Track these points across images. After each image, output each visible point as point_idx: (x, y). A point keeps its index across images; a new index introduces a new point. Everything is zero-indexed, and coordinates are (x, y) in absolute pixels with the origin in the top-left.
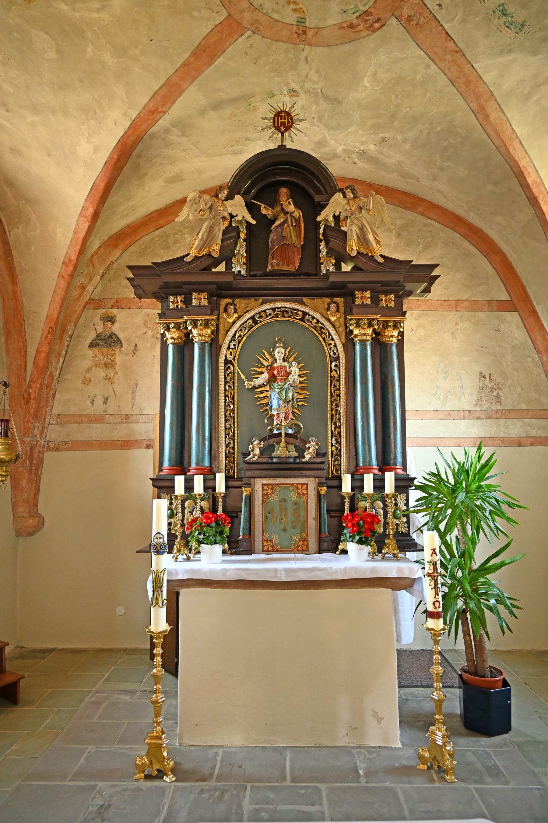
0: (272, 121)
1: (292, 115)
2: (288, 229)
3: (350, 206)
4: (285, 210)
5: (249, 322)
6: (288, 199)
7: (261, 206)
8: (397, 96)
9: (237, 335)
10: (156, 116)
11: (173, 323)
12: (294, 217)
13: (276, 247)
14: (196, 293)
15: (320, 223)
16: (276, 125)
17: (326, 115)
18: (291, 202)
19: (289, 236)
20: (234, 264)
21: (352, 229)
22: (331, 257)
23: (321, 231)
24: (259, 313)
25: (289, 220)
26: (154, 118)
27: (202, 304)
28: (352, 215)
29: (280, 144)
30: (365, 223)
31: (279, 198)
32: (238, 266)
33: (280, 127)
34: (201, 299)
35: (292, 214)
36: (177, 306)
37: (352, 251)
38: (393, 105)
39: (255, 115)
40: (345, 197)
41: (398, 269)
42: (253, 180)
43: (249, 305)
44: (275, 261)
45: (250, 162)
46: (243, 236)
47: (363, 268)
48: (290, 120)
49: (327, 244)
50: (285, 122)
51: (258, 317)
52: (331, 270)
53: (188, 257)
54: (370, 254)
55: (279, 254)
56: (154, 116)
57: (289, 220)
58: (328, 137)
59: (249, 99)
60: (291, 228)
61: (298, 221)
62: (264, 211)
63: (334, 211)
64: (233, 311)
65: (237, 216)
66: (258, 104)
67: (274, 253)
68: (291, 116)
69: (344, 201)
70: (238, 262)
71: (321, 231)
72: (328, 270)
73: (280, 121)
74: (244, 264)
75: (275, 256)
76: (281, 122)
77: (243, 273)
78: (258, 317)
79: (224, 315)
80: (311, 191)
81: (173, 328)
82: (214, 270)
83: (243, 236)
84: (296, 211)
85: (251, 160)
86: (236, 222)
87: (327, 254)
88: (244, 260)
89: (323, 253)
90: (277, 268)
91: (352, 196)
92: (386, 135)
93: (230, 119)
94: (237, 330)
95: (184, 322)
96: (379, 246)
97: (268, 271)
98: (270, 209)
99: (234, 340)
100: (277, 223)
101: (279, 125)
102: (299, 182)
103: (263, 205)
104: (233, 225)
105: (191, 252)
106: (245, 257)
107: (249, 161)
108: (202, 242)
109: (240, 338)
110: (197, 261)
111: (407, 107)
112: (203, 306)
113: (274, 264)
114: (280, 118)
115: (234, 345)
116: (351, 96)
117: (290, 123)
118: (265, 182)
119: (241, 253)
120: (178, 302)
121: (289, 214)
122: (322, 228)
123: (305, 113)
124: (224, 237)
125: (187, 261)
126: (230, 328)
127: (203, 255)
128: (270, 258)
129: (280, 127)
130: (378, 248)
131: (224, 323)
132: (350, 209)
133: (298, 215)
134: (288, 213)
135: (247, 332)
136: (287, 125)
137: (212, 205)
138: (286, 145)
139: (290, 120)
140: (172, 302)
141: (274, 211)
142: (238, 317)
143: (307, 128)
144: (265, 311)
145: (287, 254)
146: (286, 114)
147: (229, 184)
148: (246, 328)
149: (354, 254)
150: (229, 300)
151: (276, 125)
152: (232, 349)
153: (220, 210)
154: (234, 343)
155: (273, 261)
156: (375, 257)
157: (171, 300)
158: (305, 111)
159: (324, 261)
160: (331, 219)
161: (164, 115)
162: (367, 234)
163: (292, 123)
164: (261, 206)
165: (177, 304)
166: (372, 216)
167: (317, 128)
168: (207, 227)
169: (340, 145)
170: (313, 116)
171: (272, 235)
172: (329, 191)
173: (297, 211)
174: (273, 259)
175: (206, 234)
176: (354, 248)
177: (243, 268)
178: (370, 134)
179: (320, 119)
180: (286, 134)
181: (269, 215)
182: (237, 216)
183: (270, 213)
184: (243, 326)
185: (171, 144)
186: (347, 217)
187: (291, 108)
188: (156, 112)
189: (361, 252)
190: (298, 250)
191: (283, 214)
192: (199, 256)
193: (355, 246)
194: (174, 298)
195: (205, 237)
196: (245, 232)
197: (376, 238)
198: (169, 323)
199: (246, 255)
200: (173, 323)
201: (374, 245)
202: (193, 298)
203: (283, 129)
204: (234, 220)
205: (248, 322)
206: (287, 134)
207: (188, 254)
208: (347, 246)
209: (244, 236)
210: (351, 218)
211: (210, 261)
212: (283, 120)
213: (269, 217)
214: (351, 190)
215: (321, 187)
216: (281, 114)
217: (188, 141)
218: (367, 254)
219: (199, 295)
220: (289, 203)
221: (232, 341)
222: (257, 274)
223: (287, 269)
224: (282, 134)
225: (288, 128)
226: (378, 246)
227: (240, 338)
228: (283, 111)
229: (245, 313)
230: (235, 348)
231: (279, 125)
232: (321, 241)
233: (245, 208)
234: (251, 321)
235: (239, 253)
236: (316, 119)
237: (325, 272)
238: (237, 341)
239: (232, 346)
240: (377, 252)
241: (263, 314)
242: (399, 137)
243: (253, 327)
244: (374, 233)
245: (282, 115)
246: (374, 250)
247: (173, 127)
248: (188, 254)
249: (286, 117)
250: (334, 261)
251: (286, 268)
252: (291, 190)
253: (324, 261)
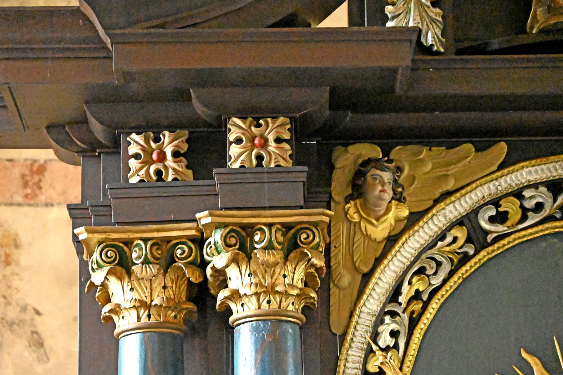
5: (455, 239)
9: (407, 292)
11: (145, 240)
14: (243, 118)
24: (496, 203)
27: (270, 164)
34: (265, 144)
36: (158, 173)
43: (453, 170)
51: (492, 220)
64: (388, 195)
78: (492, 220)
79: (352, 211)
81: (146, 262)
94: (405, 273)
95: (193, 239)
99: (393, 314)
109: (417, 306)
112: (270, 172)
115: (394, 334)
120: (162, 157)
126: (378, 261)
131: (351, 243)
135: (445, 281)
140: (137, 156)
142: (408, 218)
144: (518, 194)
148: (439, 264)
150: (375, 152)
152: (387, 349)
154: (394, 326)
157: (133, 149)
165: (160, 166)
184: (429, 253)
194: (147, 141)
198: (128, 243)
200: (145, 240)
202: (232, 137)
205: (449, 239)
219: (258, 125)
221: (387, 319)
227: (417, 306)
229: (437, 201)
230: (396, 346)
234: (461, 233)
238: (406, 317)
239: (385, 340)
241: (506, 205)
243: (465, 258)
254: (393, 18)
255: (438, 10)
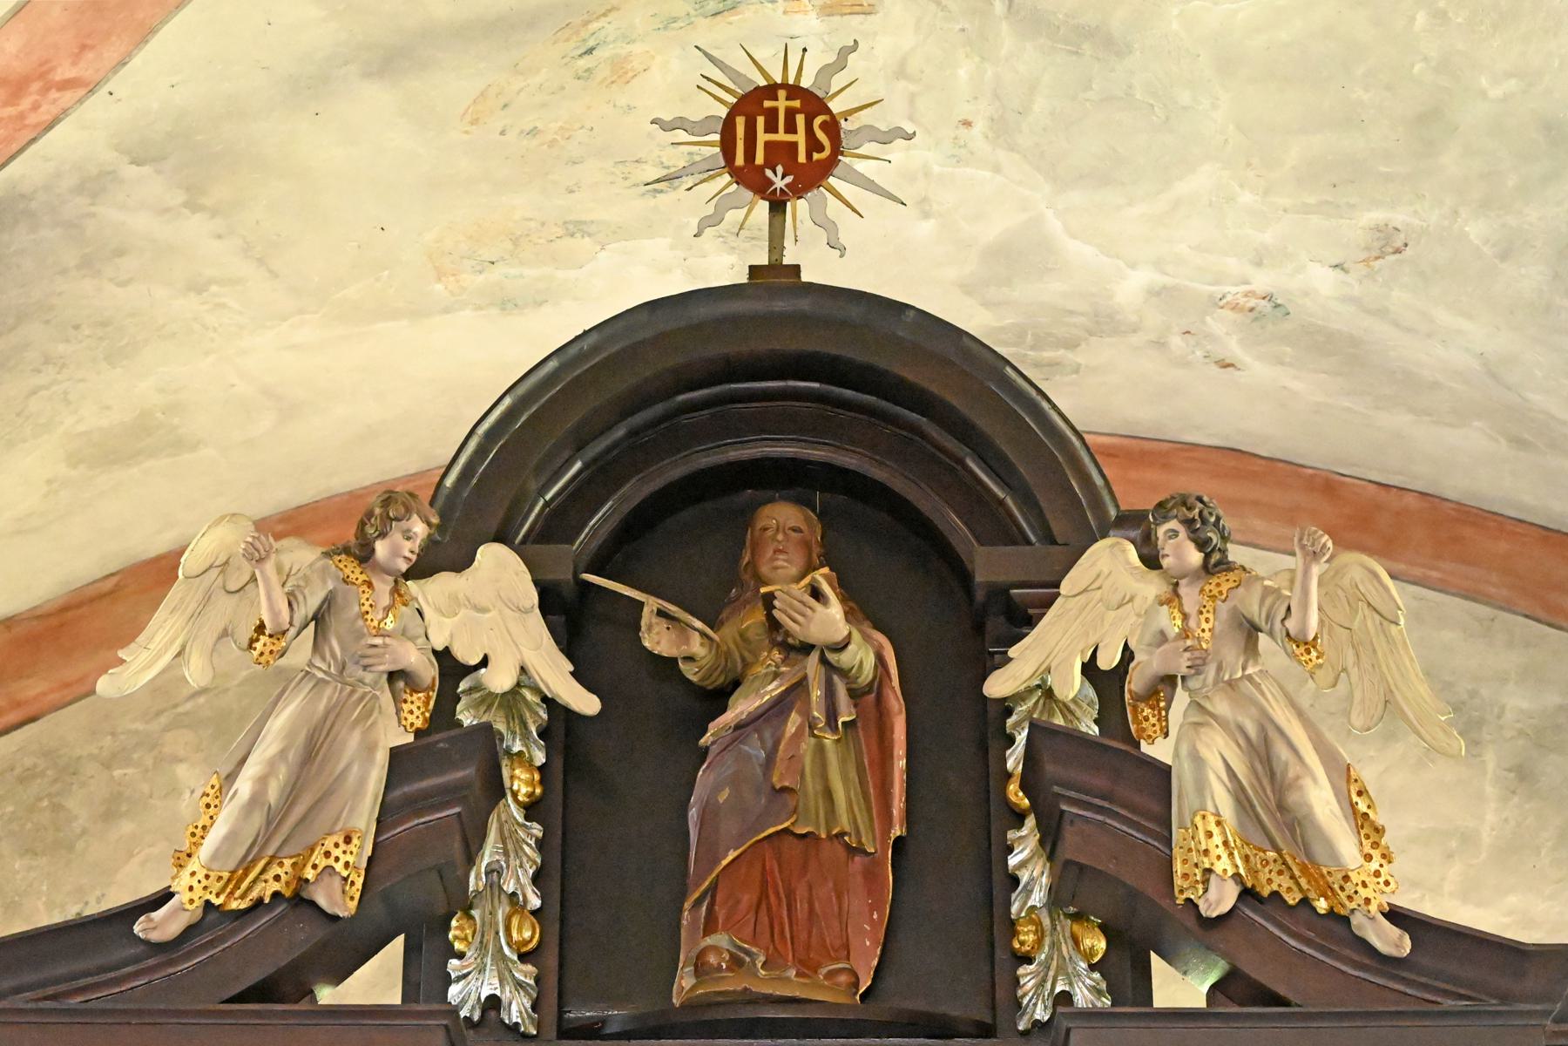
0: (717, 137)
1: (835, 106)
2: (807, 745)
3: (1185, 617)
4: (787, 634)
6: (810, 568)
7: (641, 605)
8: (1440, 16)
10: (35, 107)
12: (844, 673)
13: (732, 855)
15: (1009, 712)
16: (740, 160)
17: (1036, 108)
18: (826, 588)
19: (812, 785)
20: (461, 956)
21: (1204, 752)
22: (1077, 917)
23: (1014, 759)
25: (817, 693)
26: (22, 116)
28: (1197, 668)
29: (763, 260)
30: (1282, 716)
31: (753, 564)
32: (481, 970)
33: (761, 169)
35: (832, 657)
37: (1206, 882)
38: (1425, 59)
39: (623, 101)
40: (1151, 561)
41: (1504, 998)
42: (595, 460)
44: (721, 939)
45: (582, 357)
46: (522, 783)
47: (1282, 990)
48: (821, 136)
49: (1050, 841)
50: (794, 145)
52: (1083, 997)
53: (157, 915)
54: (1322, 905)
55: (747, 898)
56: (26, 104)
57: (817, 693)
58: (1054, 225)
59: (586, 23)
60: (829, 739)
61: (868, 695)
62: (657, 639)
63: (1092, 640)
65: (484, 662)
66: (637, 48)
67: (713, 888)
68: (828, 111)
69: (1151, 587)
70: (483, 946)
71: (1014, 759)
72: (1065, 998)
73: (762, 137)
74: (523, 957)
75: (721, 914)
76: (767, 144)
77: (517, 1010)
80: (953, 524)
82: (326, 995)
83: (522, 783)
84: (856, 636)
85: (585, 345)
86: (483, 700)
87: (1056, 899)
88: (527, 933)
89: (1028, 892)
90: (732, 984)
91: (1195, 557)
92: (1399, 217)
93: (474, 122)
96: (1376, 854)
97: (676, 1001)
98: (698, 624)
100: (741, 707)
101: (760, 159)
102: (878, 474)
103: (651, 604)
104: (466, 717)
105: (180, 885)
106: (534, 913)
107: (573, 351)
108: (258, 820)
110: (222, 939)
111: (1509, 75)
113: (712, 959)
114: (761, 121)
116: (1175, 11)
117: (821, 149)
118: (674, 470)
119: (510, 887)
121: (814, 657)
122: (1021, 738)
123: (912, 99)
124: (397, 793)
125: (155, 936)
127: (259, 903)
128: (694, 921)
129: (761, 169)
130: (1374, 866)
132: (1185, 633)
133: (870, 661)
134: (806, 648)
136: (802, 158)
137: (329, 602)
138: (796, 269)
139: (821, 136)
141: (728, 633)
143: (927, 174)
145: (801, 892)
146: (797, 104)
147: (449, 481)
149: (1220, 899)
151: (740, 160)
153: (380, 633)
155: (709, 941)
156: (1357, 920)
158: (912, 87)
159: (1039, 942)
160: (1071, 684)
161: (80, 101)
162: (1295, 784)
163: (837, 150)
164: (641, 605)
166: (1324, 676)
167: (988, 174)
168: (290, 735)
169: (1133, 266)
170: (965, 111)
171: (704, 778)
172: (1058, 528)
173: (867, 638)
174: (710, 927)
175: (283, 772)
176: (1219, 868)
177: (519, 985)
178: (1306, 210)
179: (1001, 130)
180: (800, 209)
181: (690, 659)
182: (484, 662)
183: (697, 647)
185: (120, 253)
186: (1169, 681)
187: (827, 71)
188: (35, 86)
189: (1266, 892)
190: (871, 876)
191: (777, 656)
192: (234, 905)
193: (1221, 851)
195: (273, 794)
196: (540, 758)
197: (1353, 806)
199: (535, 902)
201: (1348, 848)
203: (779, 183)
204: (470, 691)
206: (802, 205)
207: (166, 896)
208: (1176, 850)
209: (531, 783)
210: (1192, 684)
211: (305, 935)
212: (781, 136)
213: (690, 672)
214: (1188, 523)
215: (1009, 501)
216: (767, 104)
217: (220, 237)
218: (1305, 902)
220: (816, 593)
222: (604, 1021)
223: (797, 994)
224: (778, 207)
225: (811, 177)
226: (1369, 858)
228: (784, 86)
231: (760, 159)
232: (1018, 818)
233: (536, 620)
235: (494, 886)
236: (980, 126)
237: (1041, 1014)
240: (1363, 893)
242: (1476, 229)
244: (1344, 777)
245: (775, 111)
246: (1346, 878)
247: (136, 162)
248: (166, 896)
249: (800, 120)
250: (1101, 945)
251: (791, 984)
252: (825, 516)
253: (1039, 942)
254: (459, 979)
255: (529, 968)
